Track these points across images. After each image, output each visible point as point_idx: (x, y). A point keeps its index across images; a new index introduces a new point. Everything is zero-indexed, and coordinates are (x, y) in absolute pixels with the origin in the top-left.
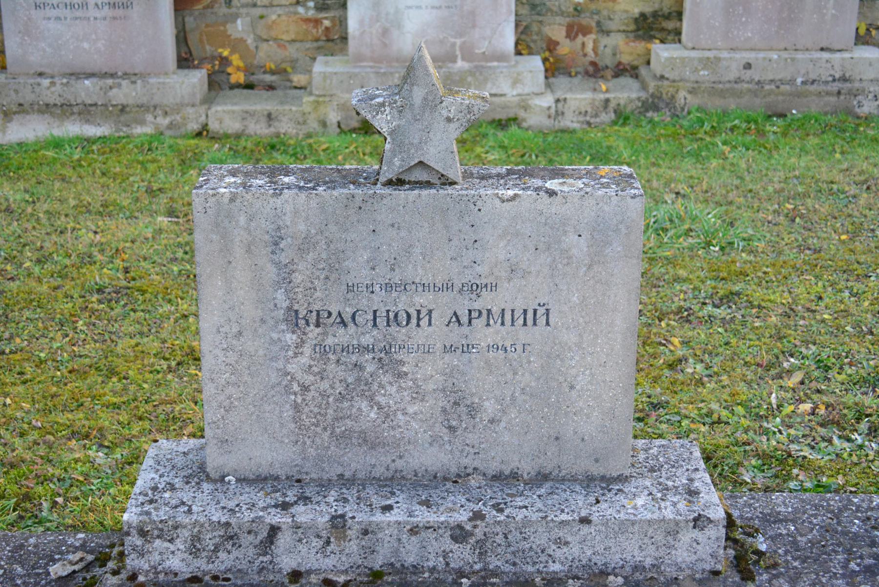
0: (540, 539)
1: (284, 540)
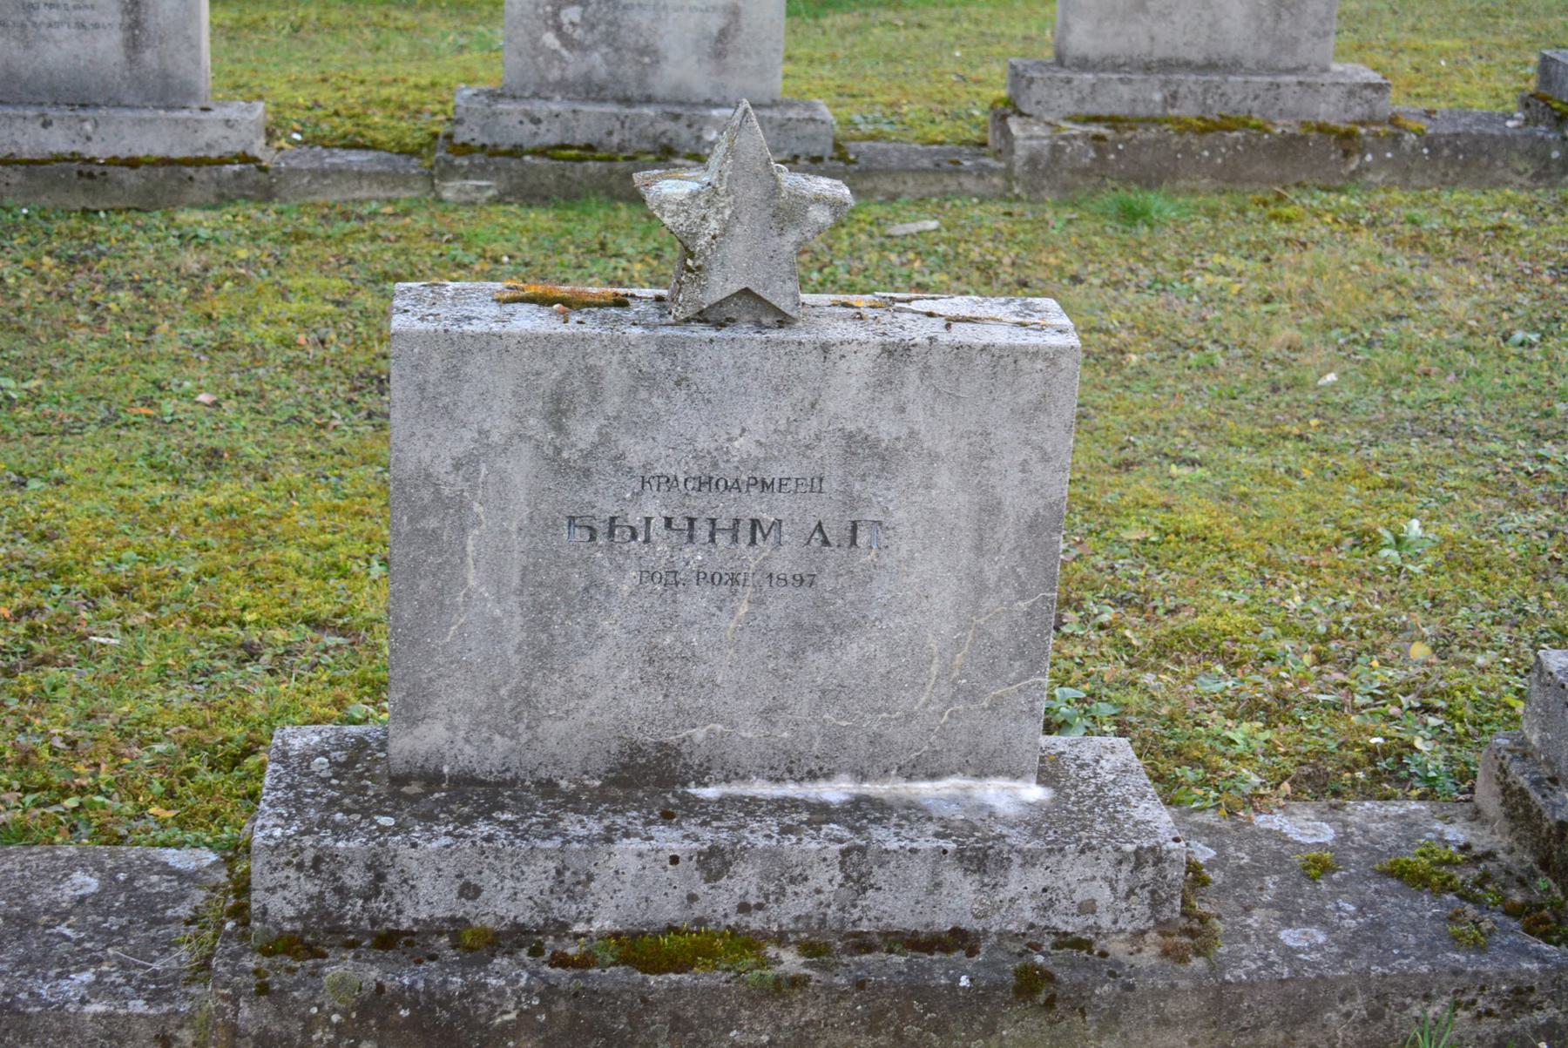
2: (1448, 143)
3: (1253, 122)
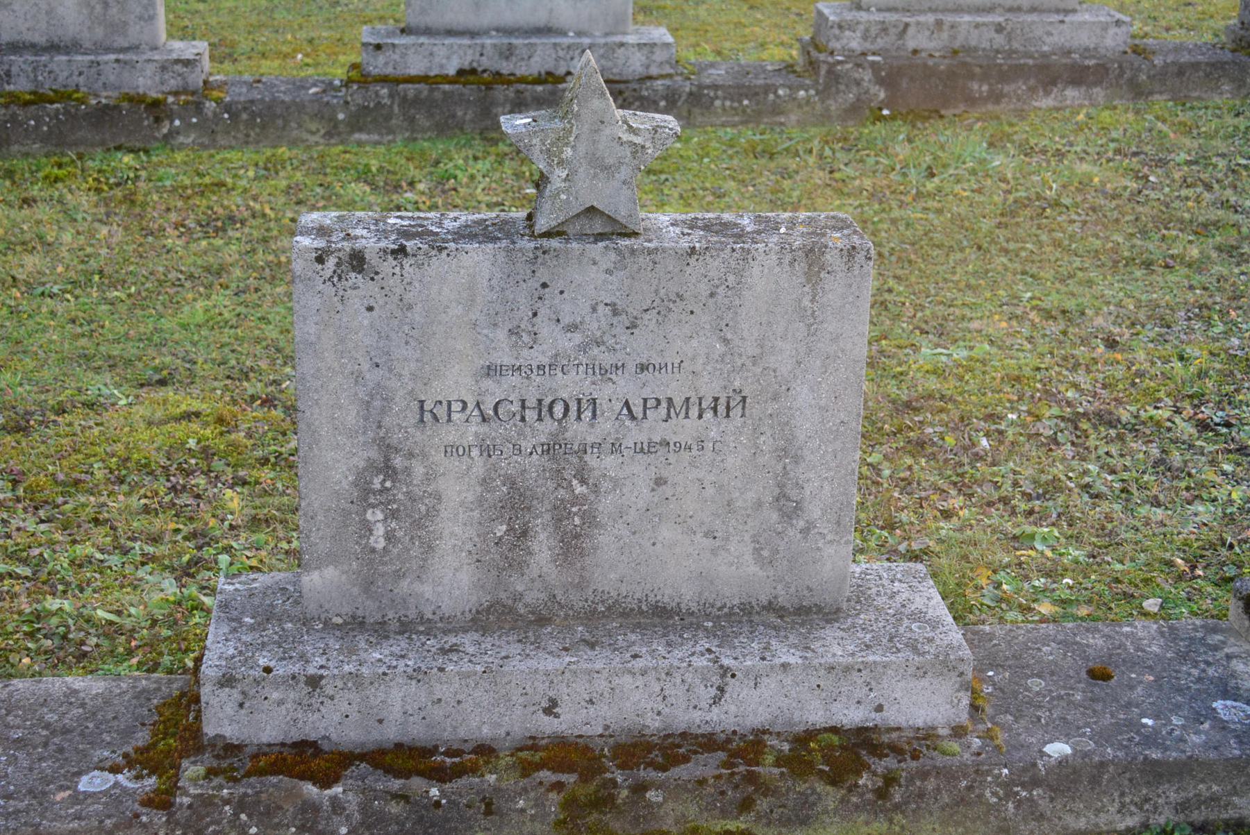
0: (1039, 32)
1: (911, 31)
2: (245, 109)
3: (76, 96)
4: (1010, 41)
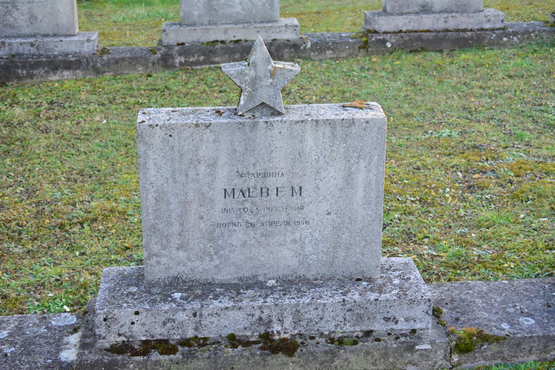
0: (51, 46)
4: (38, 50)
